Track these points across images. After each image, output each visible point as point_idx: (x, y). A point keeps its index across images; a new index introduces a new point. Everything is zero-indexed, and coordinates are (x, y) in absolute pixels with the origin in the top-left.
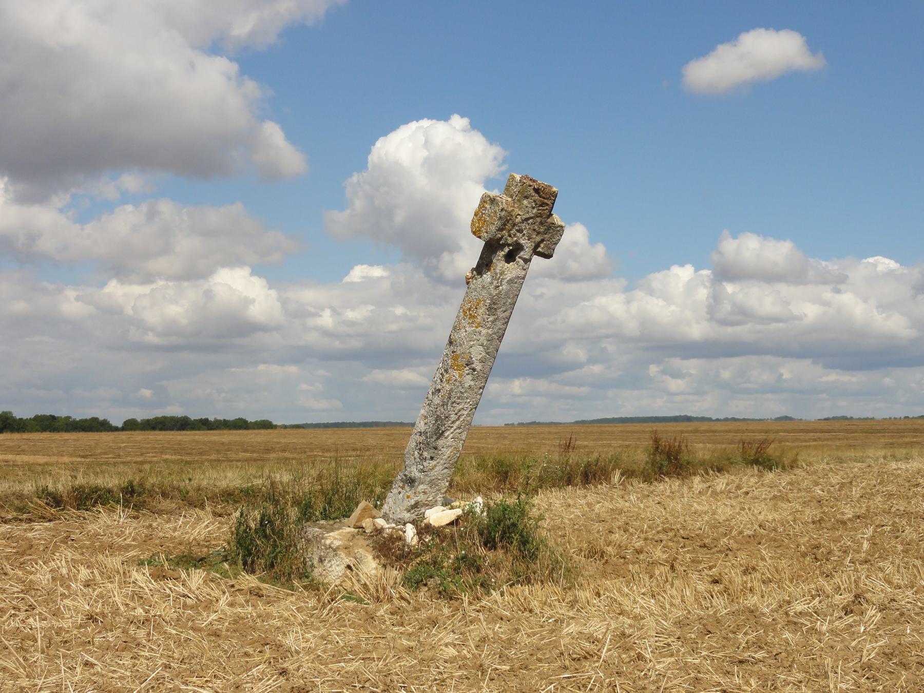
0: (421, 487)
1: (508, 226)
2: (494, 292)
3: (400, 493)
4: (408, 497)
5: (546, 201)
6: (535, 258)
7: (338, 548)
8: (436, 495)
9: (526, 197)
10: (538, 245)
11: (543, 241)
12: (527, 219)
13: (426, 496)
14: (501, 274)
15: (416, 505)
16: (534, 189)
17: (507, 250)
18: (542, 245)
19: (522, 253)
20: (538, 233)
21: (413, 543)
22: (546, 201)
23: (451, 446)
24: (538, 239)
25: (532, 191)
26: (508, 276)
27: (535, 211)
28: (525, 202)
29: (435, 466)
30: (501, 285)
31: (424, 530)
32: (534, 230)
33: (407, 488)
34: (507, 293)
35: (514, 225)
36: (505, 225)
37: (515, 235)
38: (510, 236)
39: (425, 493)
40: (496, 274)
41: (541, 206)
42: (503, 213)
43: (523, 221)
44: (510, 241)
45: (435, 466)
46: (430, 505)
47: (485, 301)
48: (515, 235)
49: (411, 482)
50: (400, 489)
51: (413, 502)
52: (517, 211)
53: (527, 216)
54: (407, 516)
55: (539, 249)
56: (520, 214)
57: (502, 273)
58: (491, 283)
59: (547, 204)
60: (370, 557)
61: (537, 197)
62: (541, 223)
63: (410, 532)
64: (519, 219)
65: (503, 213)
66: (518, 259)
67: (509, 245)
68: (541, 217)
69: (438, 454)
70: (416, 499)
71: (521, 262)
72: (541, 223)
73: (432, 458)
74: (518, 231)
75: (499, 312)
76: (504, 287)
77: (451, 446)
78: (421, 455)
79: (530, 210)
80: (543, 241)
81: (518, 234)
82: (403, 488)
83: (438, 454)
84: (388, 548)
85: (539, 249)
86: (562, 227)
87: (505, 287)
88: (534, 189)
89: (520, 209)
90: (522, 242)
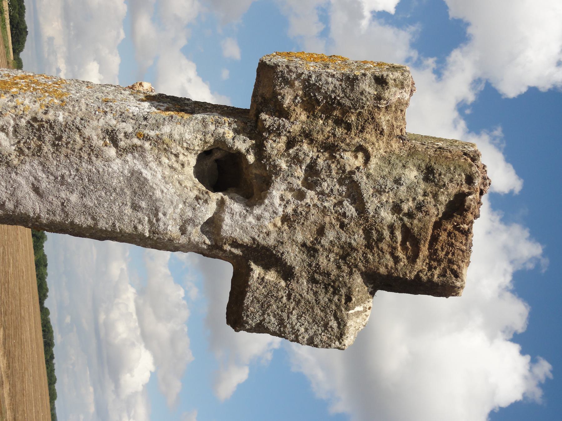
1: (324, 128)
2: (93, 132)
5: (424, 251)
6: (227, 270)
9: (429, 174)
10: (269, 257)
11: (287, 273)
12: (355, 195)
14: (158, 142)
16: (461, 198)
17: (242, 144)
18: (271, 276)
19: (237, 207)
20: (310, 250)
22: (424, 251)
24: (293, 256)
25: (453, 189)
26: (155, 173)
27: (387, 216)
28: (412, 175)
30: (122, 152)
32: (321, 231)
34: (96, 181)
35: (331, 148)
36: (328, 111)
37: (296, 160)
38: (290, 144)
40: (157, 126)
41: (407, 233)
42: (368, 87)
43: (348, 180)
44: (275, 146)
47: (62, 106)
48: (296, 160)
52: (378, 149)
53: (367, 190)
55: (257, 271)
56: (372, 162)
57: (162, 145)
58: (123, 117)
59: (413, 259)
61: (435, 211)
62: (346, 253)
64: (352, 161)
65: (368, 87)
66: (216, 196)
67: (259, 149)
68: (369, 246)
71: (208, 211)
72: (346, 253)
74: (312, 169)
75: (30, 168)
76: (116, 165)
79: (388, 198)
80: (287, 273)
81: (300, 172)
85: (257, 271)
86: (341, 336)
87: (116, 165)
88: (461, 198)
89: (387, 160)
90: (277, 191)
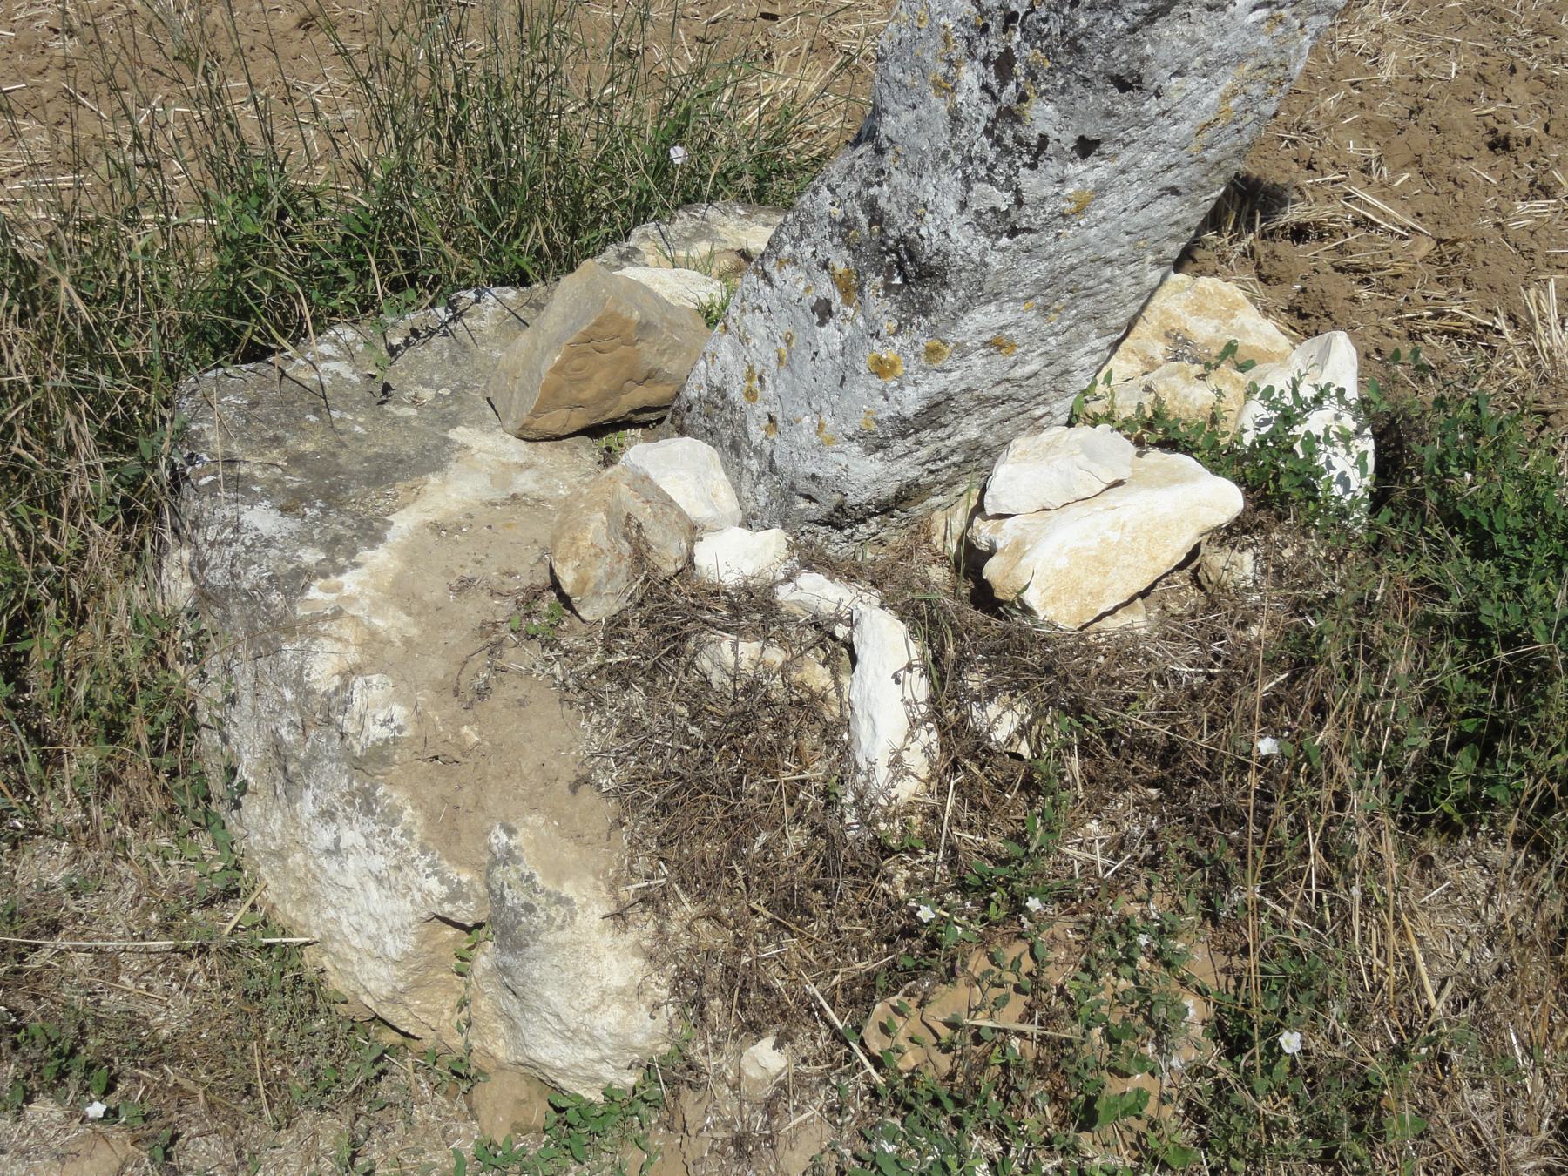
0: (983, 319)
3: (824, 311)
4: (881, 368)
7: (379, 756)
8: (1068, 346)
13: (1001, 362)
15: (934, 413)
21: (907, 790)
23: (1240, 59)
29: (1101, 190)
31: (971, 624)
33: (881, 308)
39: (998, 345)
45: (1101, 190)
46: (1017, 408)
49: (914, 274)
50: (826, 289)
51: (911, 402)
54: (867, 475)
60: (593, 909)
63: (885, 701)
69: (1139, 120)
70: (935, 384)
73: (1086, 147)
77: (1240, 59)
78: (1010, 115)
82: (851, 288)
83: (1139, 120)
84: (714, 779)
